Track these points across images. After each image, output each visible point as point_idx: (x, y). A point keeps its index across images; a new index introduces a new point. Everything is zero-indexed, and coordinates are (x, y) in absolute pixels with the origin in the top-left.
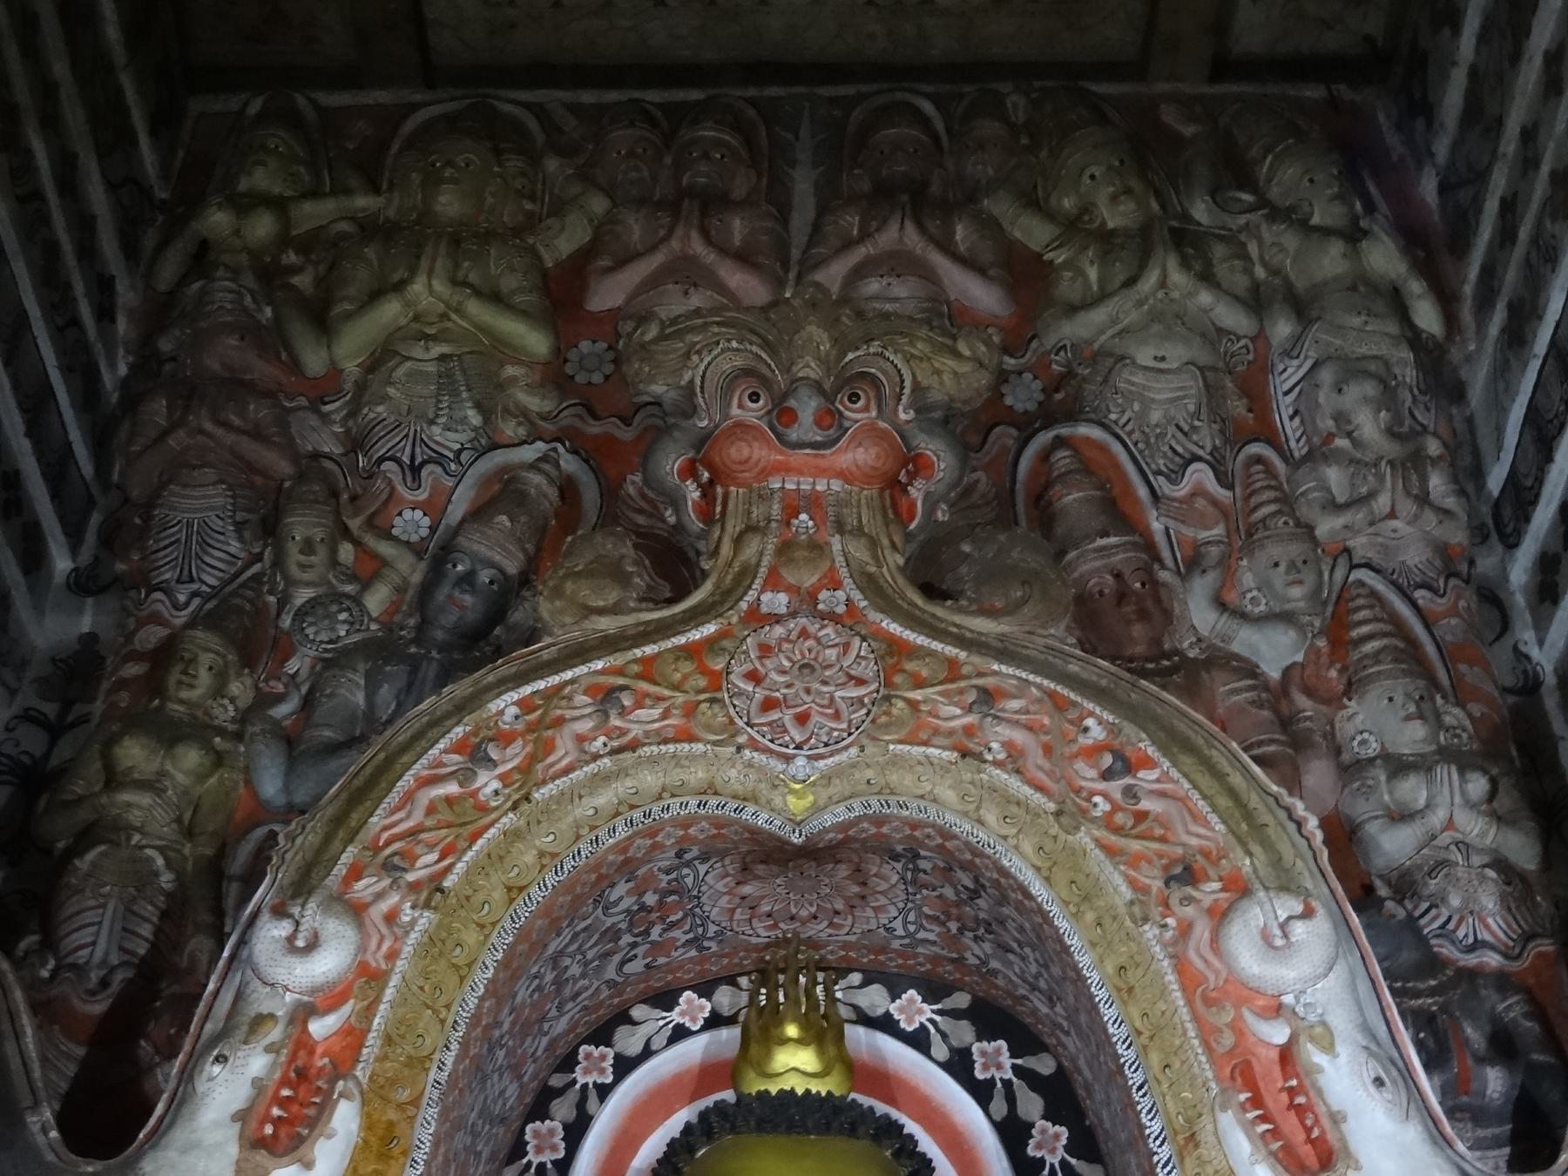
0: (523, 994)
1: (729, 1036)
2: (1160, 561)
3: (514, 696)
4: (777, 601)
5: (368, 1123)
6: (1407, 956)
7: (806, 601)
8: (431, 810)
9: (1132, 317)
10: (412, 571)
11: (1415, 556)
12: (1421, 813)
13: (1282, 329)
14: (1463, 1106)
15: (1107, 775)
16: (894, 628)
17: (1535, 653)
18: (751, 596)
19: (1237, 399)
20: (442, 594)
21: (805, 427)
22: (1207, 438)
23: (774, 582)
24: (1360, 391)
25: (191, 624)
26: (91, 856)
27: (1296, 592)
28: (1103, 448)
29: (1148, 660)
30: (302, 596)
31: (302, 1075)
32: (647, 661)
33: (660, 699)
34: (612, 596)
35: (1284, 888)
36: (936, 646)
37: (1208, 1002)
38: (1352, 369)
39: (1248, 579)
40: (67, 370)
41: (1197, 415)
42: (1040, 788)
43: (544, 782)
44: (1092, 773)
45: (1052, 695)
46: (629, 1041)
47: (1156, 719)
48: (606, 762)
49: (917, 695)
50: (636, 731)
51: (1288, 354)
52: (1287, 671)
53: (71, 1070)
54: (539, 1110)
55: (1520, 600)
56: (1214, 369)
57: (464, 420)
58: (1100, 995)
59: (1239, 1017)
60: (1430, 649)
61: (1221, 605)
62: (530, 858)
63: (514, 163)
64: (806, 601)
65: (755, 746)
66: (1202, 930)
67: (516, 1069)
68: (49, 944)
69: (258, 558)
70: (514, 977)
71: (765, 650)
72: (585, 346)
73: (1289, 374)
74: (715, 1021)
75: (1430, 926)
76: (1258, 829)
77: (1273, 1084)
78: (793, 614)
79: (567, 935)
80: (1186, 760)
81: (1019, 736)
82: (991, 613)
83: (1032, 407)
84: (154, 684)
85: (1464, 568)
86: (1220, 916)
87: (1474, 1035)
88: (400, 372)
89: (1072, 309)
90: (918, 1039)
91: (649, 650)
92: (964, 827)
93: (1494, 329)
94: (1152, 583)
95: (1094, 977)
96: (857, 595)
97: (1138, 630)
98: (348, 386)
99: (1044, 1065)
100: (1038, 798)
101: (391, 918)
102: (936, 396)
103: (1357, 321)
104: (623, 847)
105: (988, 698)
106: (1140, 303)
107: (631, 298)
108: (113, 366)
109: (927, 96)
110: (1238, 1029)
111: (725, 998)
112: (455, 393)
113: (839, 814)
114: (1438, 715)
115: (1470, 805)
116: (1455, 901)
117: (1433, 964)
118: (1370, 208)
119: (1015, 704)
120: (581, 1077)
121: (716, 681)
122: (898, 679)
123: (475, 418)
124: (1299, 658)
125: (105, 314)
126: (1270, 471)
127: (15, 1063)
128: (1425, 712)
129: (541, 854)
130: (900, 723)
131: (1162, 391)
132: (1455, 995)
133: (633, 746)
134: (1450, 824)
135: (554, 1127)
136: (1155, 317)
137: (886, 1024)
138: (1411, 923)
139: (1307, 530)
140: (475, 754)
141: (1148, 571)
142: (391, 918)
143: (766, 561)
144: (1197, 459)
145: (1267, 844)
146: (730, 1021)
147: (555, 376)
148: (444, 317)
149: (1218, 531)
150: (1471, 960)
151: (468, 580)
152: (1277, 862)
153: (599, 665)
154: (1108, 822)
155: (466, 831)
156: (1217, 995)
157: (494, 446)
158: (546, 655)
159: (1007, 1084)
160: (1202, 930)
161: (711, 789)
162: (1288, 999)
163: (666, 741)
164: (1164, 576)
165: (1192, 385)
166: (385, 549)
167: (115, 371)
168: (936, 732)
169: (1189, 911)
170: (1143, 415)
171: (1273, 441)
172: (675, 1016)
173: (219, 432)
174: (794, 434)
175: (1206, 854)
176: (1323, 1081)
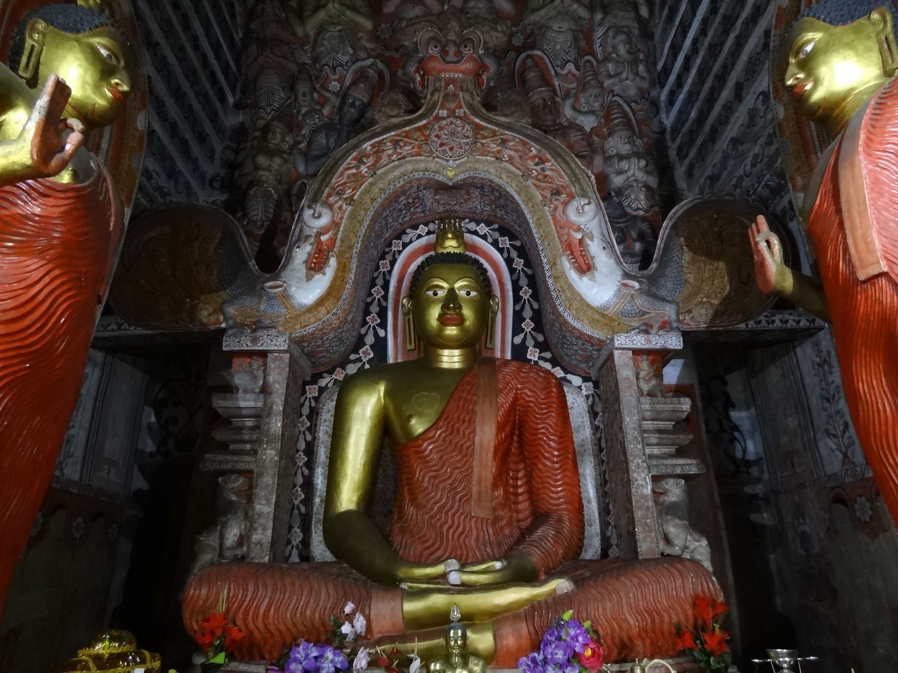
0: (377, 228)
1: (433, 237)
3: (369, 143)
4: (444, 113)
5: (339, 263)
6: (618, 212)
7: (452, 113)
8: (349, 177)
9: (552, 13)
10: (335, 101)
11: (632, 92)
12: (626, 171)
13: (599, 16)
14: (627, 253)
15: (536, 164)
16: (478, 121)
17: (665, 121)
18: (436, 112)
19: (583, 38)
20: (345, 109)
21: (451, 57)
22: (573, 55)
23: (443, 107)
24: (620, 38)
25: (273, 119)
26: (253, 190)
27: (597, 104)
28: (541, 58)
30: (304, 110)
31: (320, 251)
32: (406, 132)
33: (411, 143)
34: (396, 112)
35: (583, 196)
36: (489, 126)
37: (561, 228)
38: (619, 30)
39: (583, 100)
40: (224, 36)
41: (570, 47)
42: (518, 168)
44: (532, 164)
45: (522, 140)
46: (406, 239)
49: (484, 141)
50: (405, 153)
51: (600, 25)
52: (592, 129)
53: (256, 249)
54: (383, 257)
55: (663, 104)
56: (577, 31)
58: (532, 226)
60: (634, 121)
61: (574, 108)
62: (377, 190)
64: (452, 113)
65: (438, 157)
66: (560, 208)
67: (376, 247)
68: (245, 215)
69: (290, 98)
70: (374, 223)
71: (441, 128)
72: (383, 25)
73: (600, 32)
75: (625, 204)
76: (578, 179)
77: (577, 249)
78: (448, 117)
79: (388, 211)
80: (559, 159)
81: (512, 153)
82: (506, 116)
83: (520, 44)
84: (264, 138)
85: (646, 96)
86: (565, 204)
87: (634, 234)
88: (327, 36)
89: (534, 11)
90: (484, 237)
91: (407, 128)
92: (496, 180)
94: (554, 102)
95: (531, 221)
96: (467, 111)
97: (549, 117)
98: (311, 40)
100: (517, 171)
101: (340, 208)
102: (491, 45)
103: (622, 13)
104: (402, 187)
106: (555, 8)
108: (238, 34)
110: (569, 235)
111: (432, 226)
112: (344, 43)
113: (462, 176)
114: (634, 142)
115: (639, 169)
116: (633, 197)
117: (625, 214)
119: (511, 144)
121: (427, 137)
122: (479, 136)
123: (351, 52)
125: (233, 16)
126: (592, 65)
127: (243, 249)
128: (631, 141)
129: (380, 189)
130: (479, 149)
131: (561, 38)
132: (630, 223)
133: (404, 158)
134: (634, 175)
136: (560, 13)
137: (475, 233)
138: (620, 203)
139: (601, 84)
140: (360, 161)
142: (340, 208)
144: (569, 61)
145: (580, 184)
146: (433, 233)
147: (375, 36)
148: (339, 16)
149: (575, 85)
150: (635, 213)
151: (352, 105)
152: (582, 189)
153: (393, 133)
156: (563, 226)
157: (357, 60)
158: (378, 130)
160: (560, 208)
161: (426, 170)
162: (582, 227)
164: (558, 100)
165: (570, 36)
166: (327, 94)
167: (238, 35)
168: (489, 152)
169: (557, 203)
170: (554, 47)
171: (594, 55)
172: (418, 232)
173: (274, 57)
174: (448, 59)
175: (563, 187)
176: (589, 248)
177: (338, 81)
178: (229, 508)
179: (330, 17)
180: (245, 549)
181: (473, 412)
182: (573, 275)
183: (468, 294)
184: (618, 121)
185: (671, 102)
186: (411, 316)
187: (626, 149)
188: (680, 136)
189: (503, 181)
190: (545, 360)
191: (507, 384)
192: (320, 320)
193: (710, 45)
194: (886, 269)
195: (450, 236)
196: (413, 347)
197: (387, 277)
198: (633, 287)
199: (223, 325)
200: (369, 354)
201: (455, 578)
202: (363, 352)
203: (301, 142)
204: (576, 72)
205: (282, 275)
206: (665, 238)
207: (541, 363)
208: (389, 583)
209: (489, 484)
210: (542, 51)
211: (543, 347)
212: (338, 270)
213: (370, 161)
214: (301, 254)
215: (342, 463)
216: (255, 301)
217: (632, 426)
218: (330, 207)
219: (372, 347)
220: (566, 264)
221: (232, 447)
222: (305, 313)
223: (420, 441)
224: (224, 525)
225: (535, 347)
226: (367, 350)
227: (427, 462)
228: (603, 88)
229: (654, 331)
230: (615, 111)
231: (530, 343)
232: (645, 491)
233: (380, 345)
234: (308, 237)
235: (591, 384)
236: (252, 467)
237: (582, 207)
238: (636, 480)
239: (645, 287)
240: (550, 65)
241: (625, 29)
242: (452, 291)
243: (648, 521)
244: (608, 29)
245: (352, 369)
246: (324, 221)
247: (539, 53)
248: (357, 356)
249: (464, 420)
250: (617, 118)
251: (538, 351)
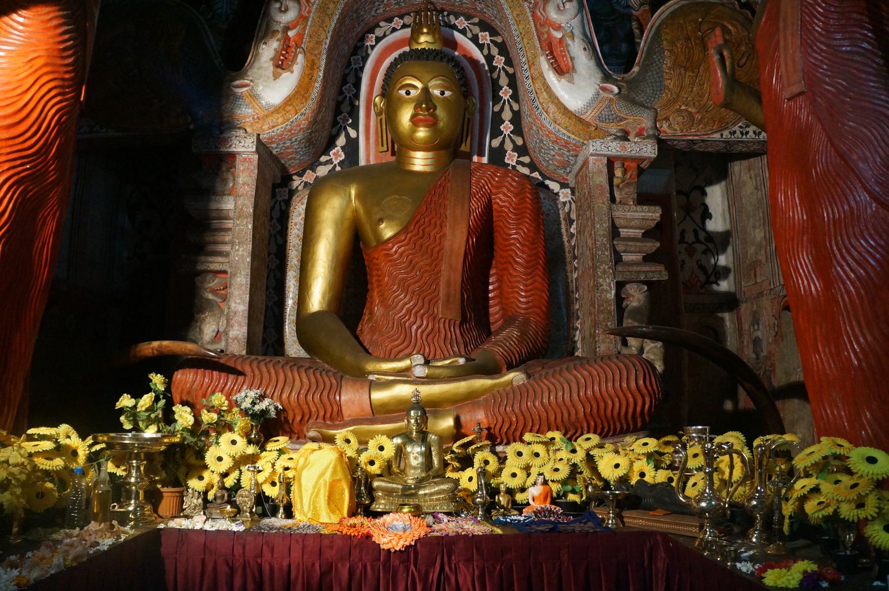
1: (408, 31)
37: (541, 25)
46: (379, 32)
59: (549, 30)
74: (404, 26)
99: (499, 40)
110: (548, 33)
111: (408, 20)
146: (408, 26)
156: (543, 24)
159: (488, 45)
172: (393, 25)
183: (443, 93)
186: (383, 116)
190: (523, 164)
195: (425, 30)
198: (612, 92)
199: (191, 127)
200: (340, 156)
202: (334, 154)
205: (249, 73)
206: (649, 40)
207: (520, 168)
208: (360, 375)
211: (522, 150)
214: (267, 51)
215: (313, 266)
217: (601, 233)
219: (342, 147)
220: (544, 65)
225: (513, 150)
226: (338, 151)
231: (509, 146)
233: (352, 147)
234: (276, 32)
235: (569, 191)
238: (601, 285)
242: (426, 90)
243: (609, 323)
245: (322, 171)
248: (328, 158)
251: (516, 154)
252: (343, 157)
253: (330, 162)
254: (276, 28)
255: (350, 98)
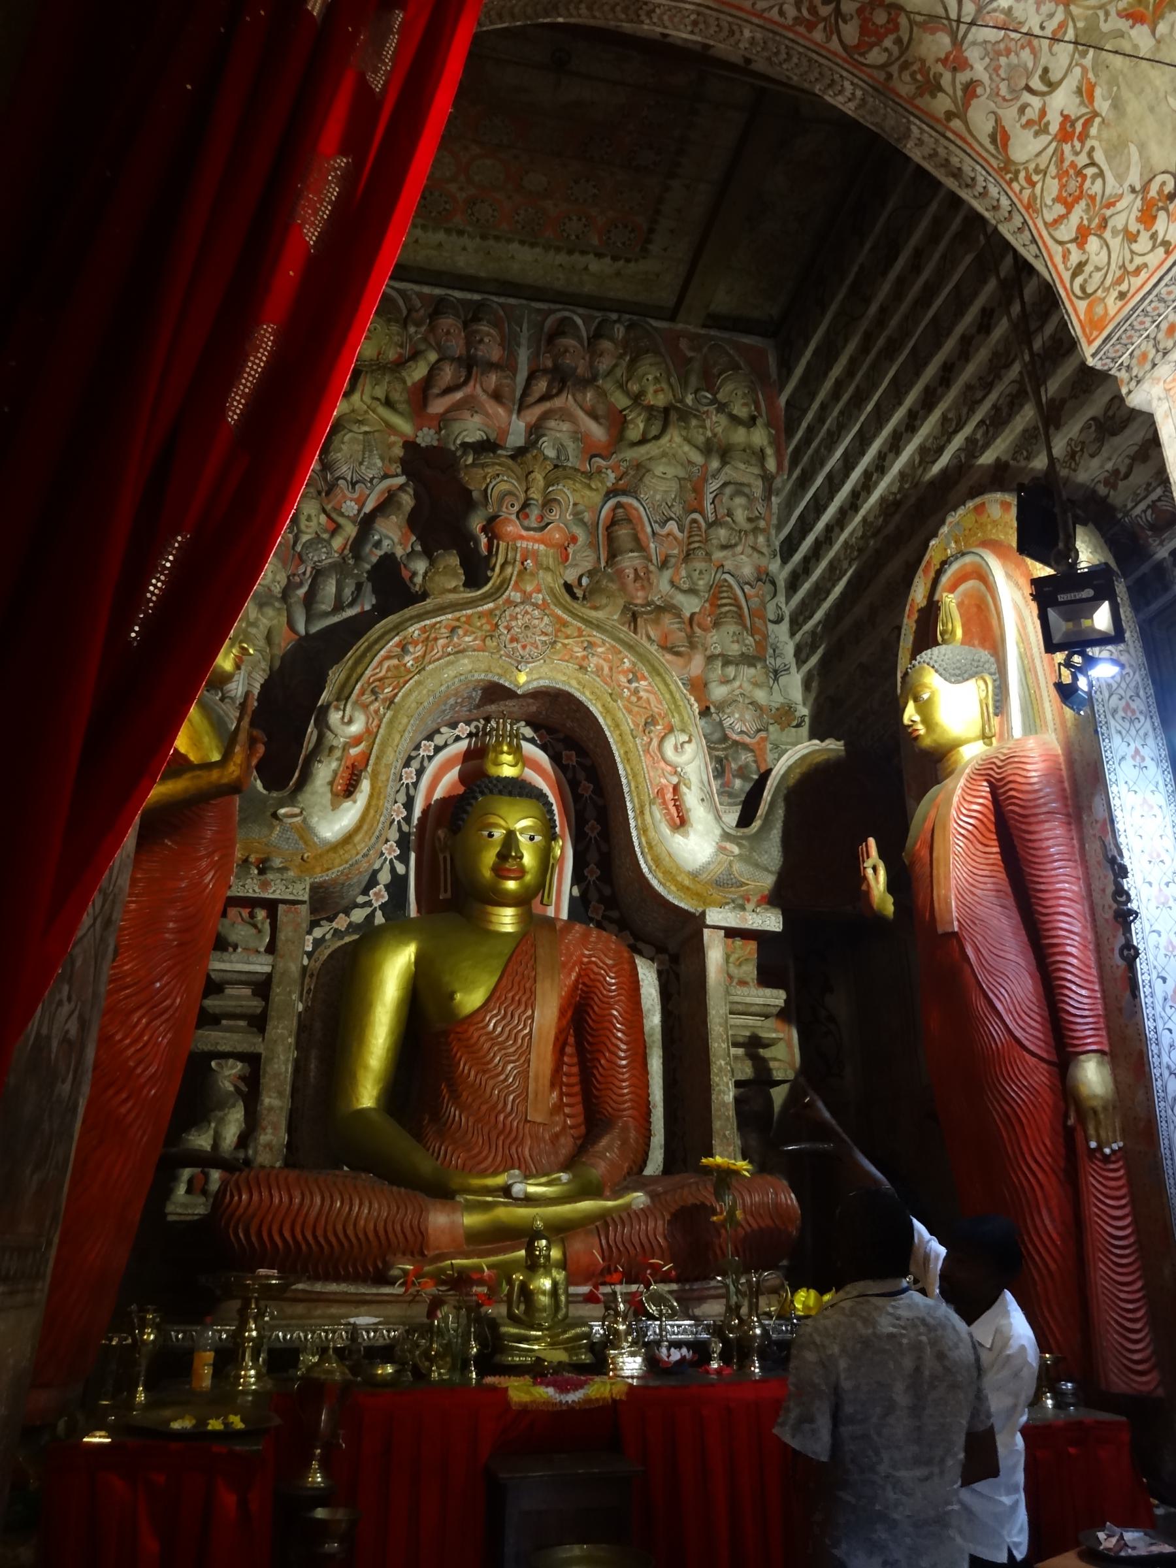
2: (651, 561)
4: (517, 596)
5: (373, 787)
6: (717, 736)
7: (526, 598)
8: (388, 669)
10: (351, 530)
13: (715, 464)
14: (726, 792)
16: (560, 612)
17: (783, 606)
18: (507, 593)
22: (678, 509)
23: (517, 587)
24: (740, 501)
28: (636, 509)
29: (643, 606)
30: (305, 538)
32: (469, 617)
34: (453, 584)
35: (683, 731)
38: (740, 489)
41: (674, 500)
43: (430, 663)
45: (614, 647)
46: (439, 740)
47: (648, 661)
48: (452, 657)
49: (566, 641)
51: (714, 476)
52: (693, 615)
54: (407, 764)
56: (684, 479)
57: (375, 464)
60: (746, 610)
62: (425, 692)
63: (395, 328)
75: (726, 723)
76: (677, 707)
78: (522, 603)
80: (658, 679)
81: (601, 661)
88: (346, 438)
91: (469, 612)
92: (577, 694)
93: (795, 476)
94: (648, 572)
97: (640, 594)
101: (377, 712)
103: (742, 466)
105: (591, 645)
107: (448, 411)
109: (580, 316)
112: (371, 451)
113: (535, 684)
114: (744, 640)
116: (737, 716)
117: (725, 738)
118: (757, 408)
119: (600, 650)
120: (422, 753)
123: (379, 463)
124: (697, 610)
126: (699, 528)
130: (559, 652)
131: (662, 486)
132: (730, 751)
134: (740, 687)
135: (412, 770)
136: (664, 454)
138: (721, 723)
140: (404, 649)
141: (647, 567)
142: (377, 712)
143: (514, 578)
144: (671, 519)
145: (680, 714)
148: (366, 412)
152: (682, 721)
153: (450, 616)
154: (628, 700)
155: (402, 680)
157: (386, 476)
163: (474, 650)
164: (652, 568)
165: (675, 486)
170: (653, 496)
171: (702, 512)
172: (457, 732)
174: (526, 523)
175: (660, 715)
177: (357, 501)
178: (222, 1104)
179: (353, 411)
180: (250, 1152)
181: (533, 993)
182: (666, 830)
184: (727, 608)
185: (793, 585)
187: (734, 649)
188: (801, 633)
189: (584, 697)
191: (571, 956)
192: (347, 862)
193: (846, 542)
194: (956, 929)
195: (505, 748)
196: (449, 895)
197: (412, 791)
200: (383, 897)
201: (518, 1189)
202: (375, 894)
203: (301, 584)
204: (679, 535)
205: (299, 798)
209: (547, 1083)
210: (638, 500)
212: (371, 796)
213: (419, 650)
214: (325, 772)
216: (265, 831)
217: (717, 1020)
218: (365, 707)
219: (387, 887)
221: (224, 1022)
222: (328, 851)
223: (466, 1026)
224: (221, 1121)
226: (380, 890)
227: (473, 1053)
228: (711, 559)
229: (750, 906)
230: (725, 595)
232: (726, 1097)
236: (261, 1049)
237: (682, 745)
239: (744, 851)
240: (645, 519)
241: (746, 490)
243: (727, 1133)
244: (725, 485)
246: (355, 729)
247: (636, 503)
248: (366, 899)
249: (519, 1001)
250: (725, 605)
252: (386, 898)
253: (369, 904)
254: (335, 743)
255: (399, 822)
